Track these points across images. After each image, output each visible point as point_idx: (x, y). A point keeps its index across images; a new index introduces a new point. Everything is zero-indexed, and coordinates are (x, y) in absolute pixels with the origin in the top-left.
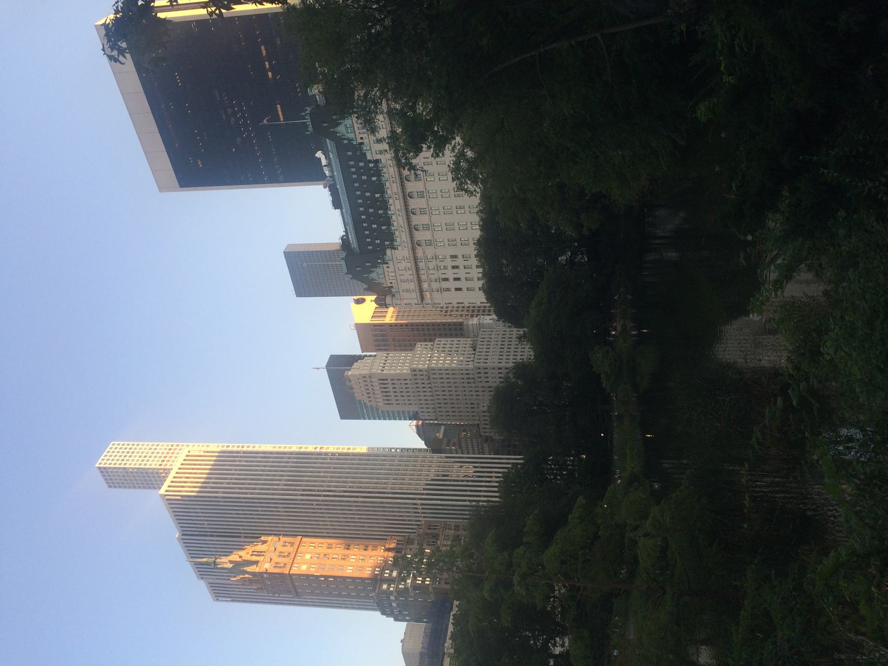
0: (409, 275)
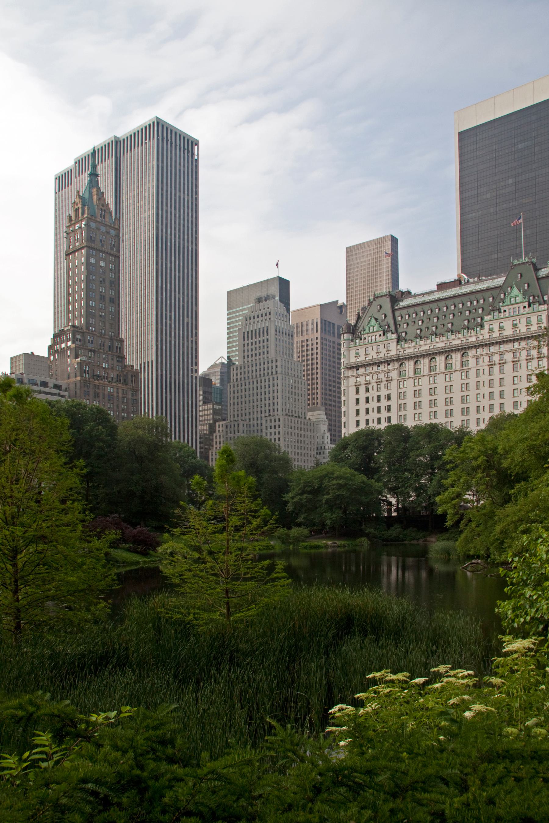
0: (373, 355)
